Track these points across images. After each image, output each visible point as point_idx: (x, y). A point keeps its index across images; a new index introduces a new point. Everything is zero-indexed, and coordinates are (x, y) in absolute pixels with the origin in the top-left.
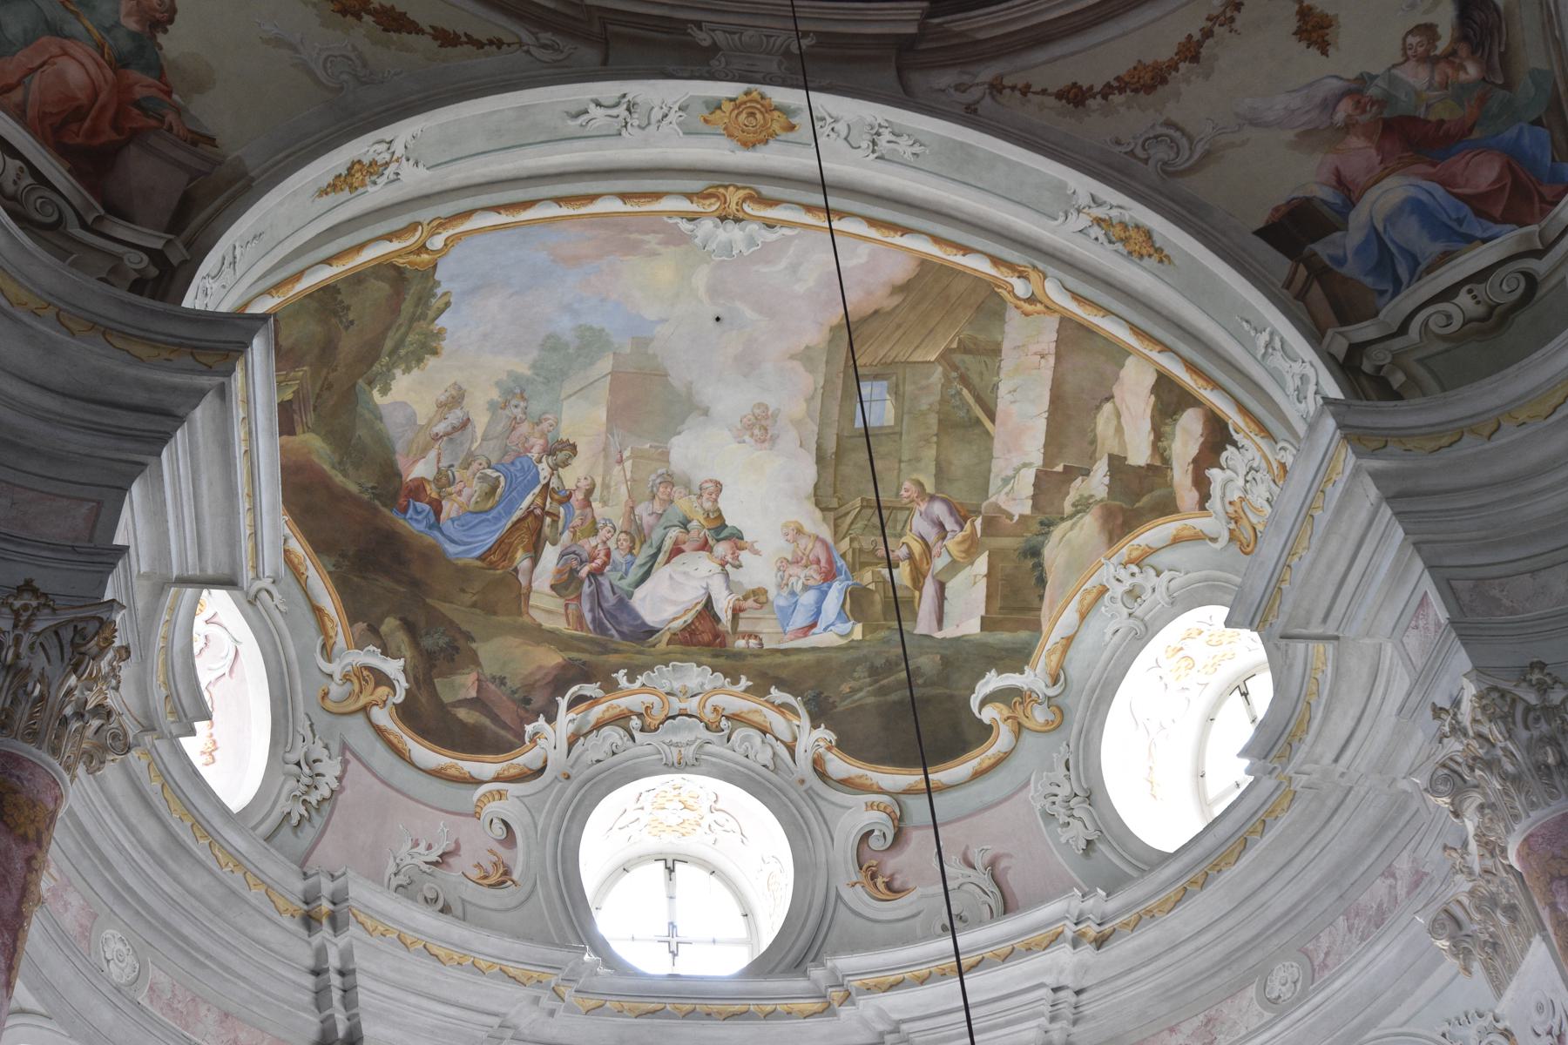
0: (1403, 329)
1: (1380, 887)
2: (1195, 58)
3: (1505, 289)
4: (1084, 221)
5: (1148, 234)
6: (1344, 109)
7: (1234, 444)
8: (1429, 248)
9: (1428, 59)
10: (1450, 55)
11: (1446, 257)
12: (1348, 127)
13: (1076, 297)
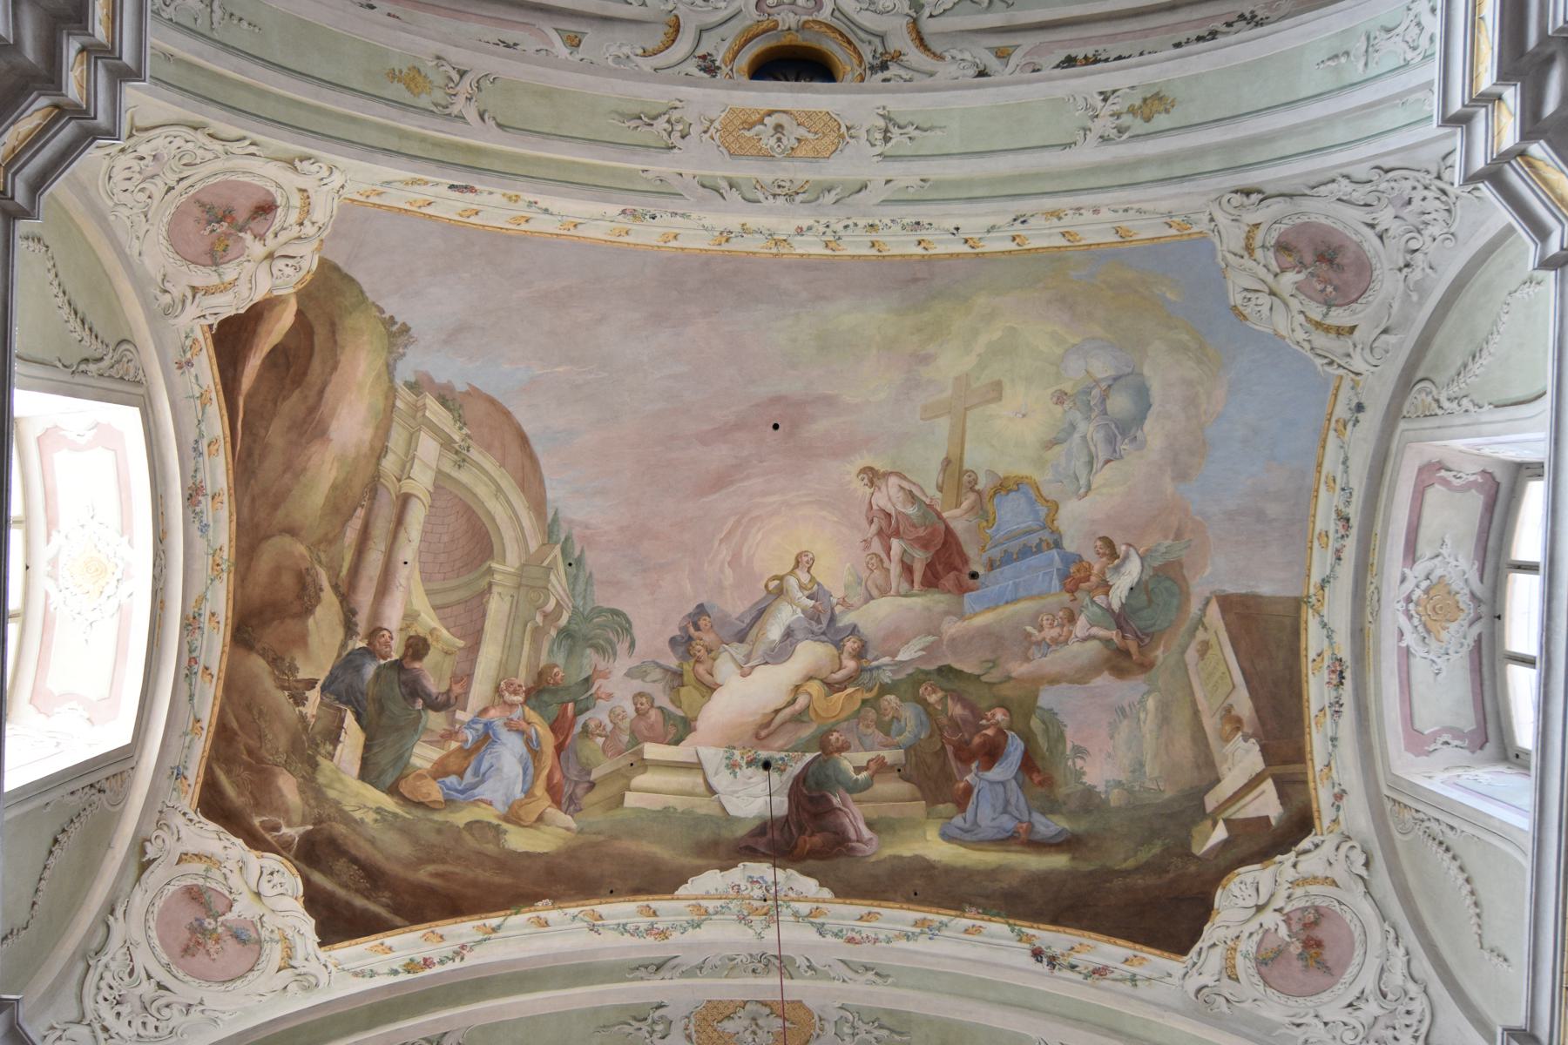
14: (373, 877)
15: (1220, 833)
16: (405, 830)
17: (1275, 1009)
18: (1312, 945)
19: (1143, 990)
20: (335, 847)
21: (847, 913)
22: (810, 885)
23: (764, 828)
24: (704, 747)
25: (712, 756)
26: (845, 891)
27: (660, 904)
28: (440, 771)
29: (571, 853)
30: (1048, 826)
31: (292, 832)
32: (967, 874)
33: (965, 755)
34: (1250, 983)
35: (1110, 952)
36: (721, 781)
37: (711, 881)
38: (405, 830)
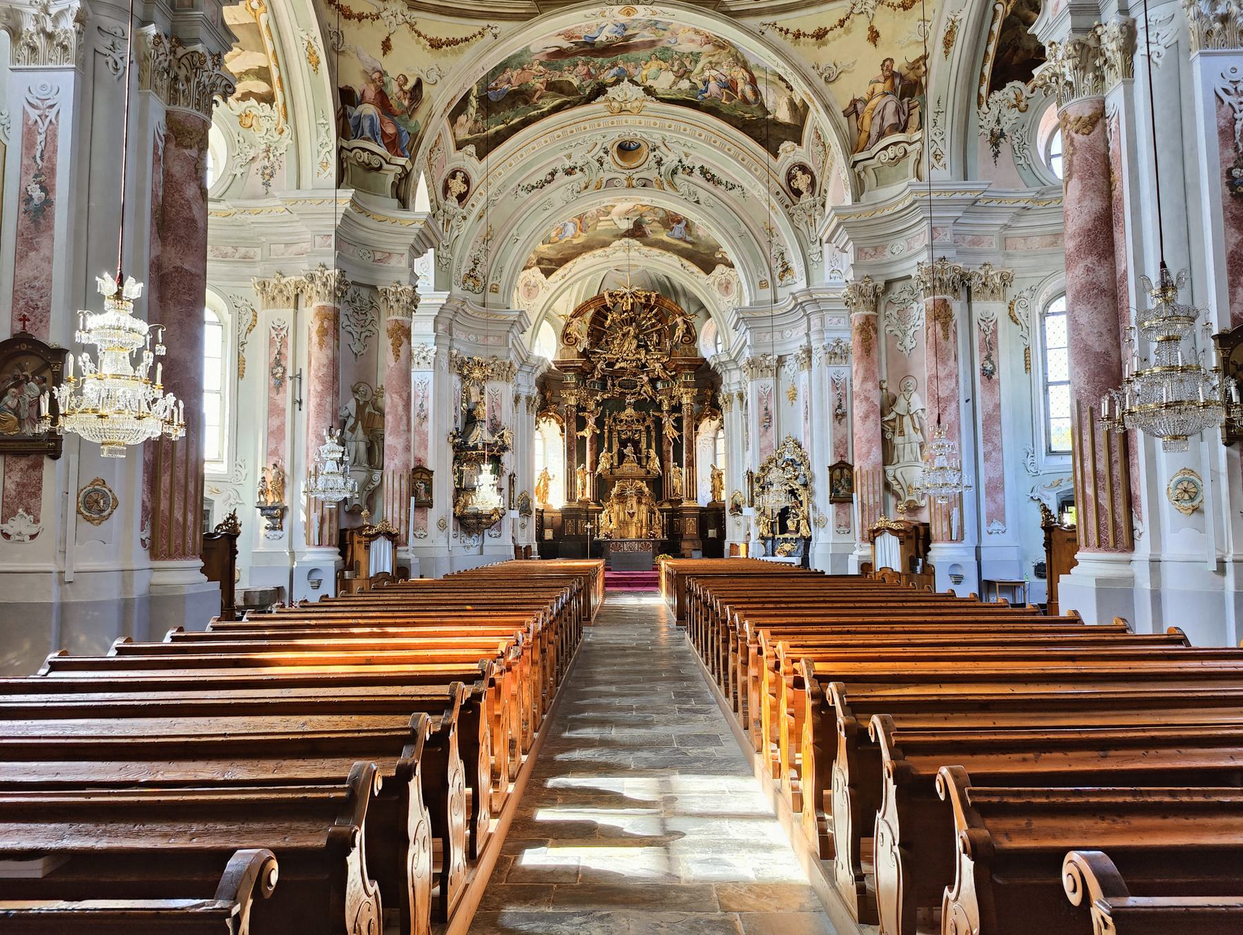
0: (351, 151)
1: (230, 250)
2: (360, 21)
3: (375, 164)
4: (306, 37)
5: (318, 63)
6: (376, 75)
7: (272, 108)
8: (368, 134)
9: (400, 86)
10: (405, 93)
11: (368, 139)
12: (373, 81)
13: (268, 26)
14: (550, 261)
15: (720, 256)
16: (554, 249)
17: (718, 295)
18: (727, 287)
19: (699, 280)
20: (542, 259)
21: (645, 249)
22: (638, 243)
23: (628, 231)
24: (614, 216)
25: (616, 218)
26: (646, 244)
27: (606, 249)
28: (557, 235)
29: (587, 241)
30: (689, 238)
31: (535, 261)
32: (671, 244)
33: (673, 221)
34: (715, 288)
35: (695, 269)
36: (618, 222)
37: (617, 243)
38: (554, 249)
